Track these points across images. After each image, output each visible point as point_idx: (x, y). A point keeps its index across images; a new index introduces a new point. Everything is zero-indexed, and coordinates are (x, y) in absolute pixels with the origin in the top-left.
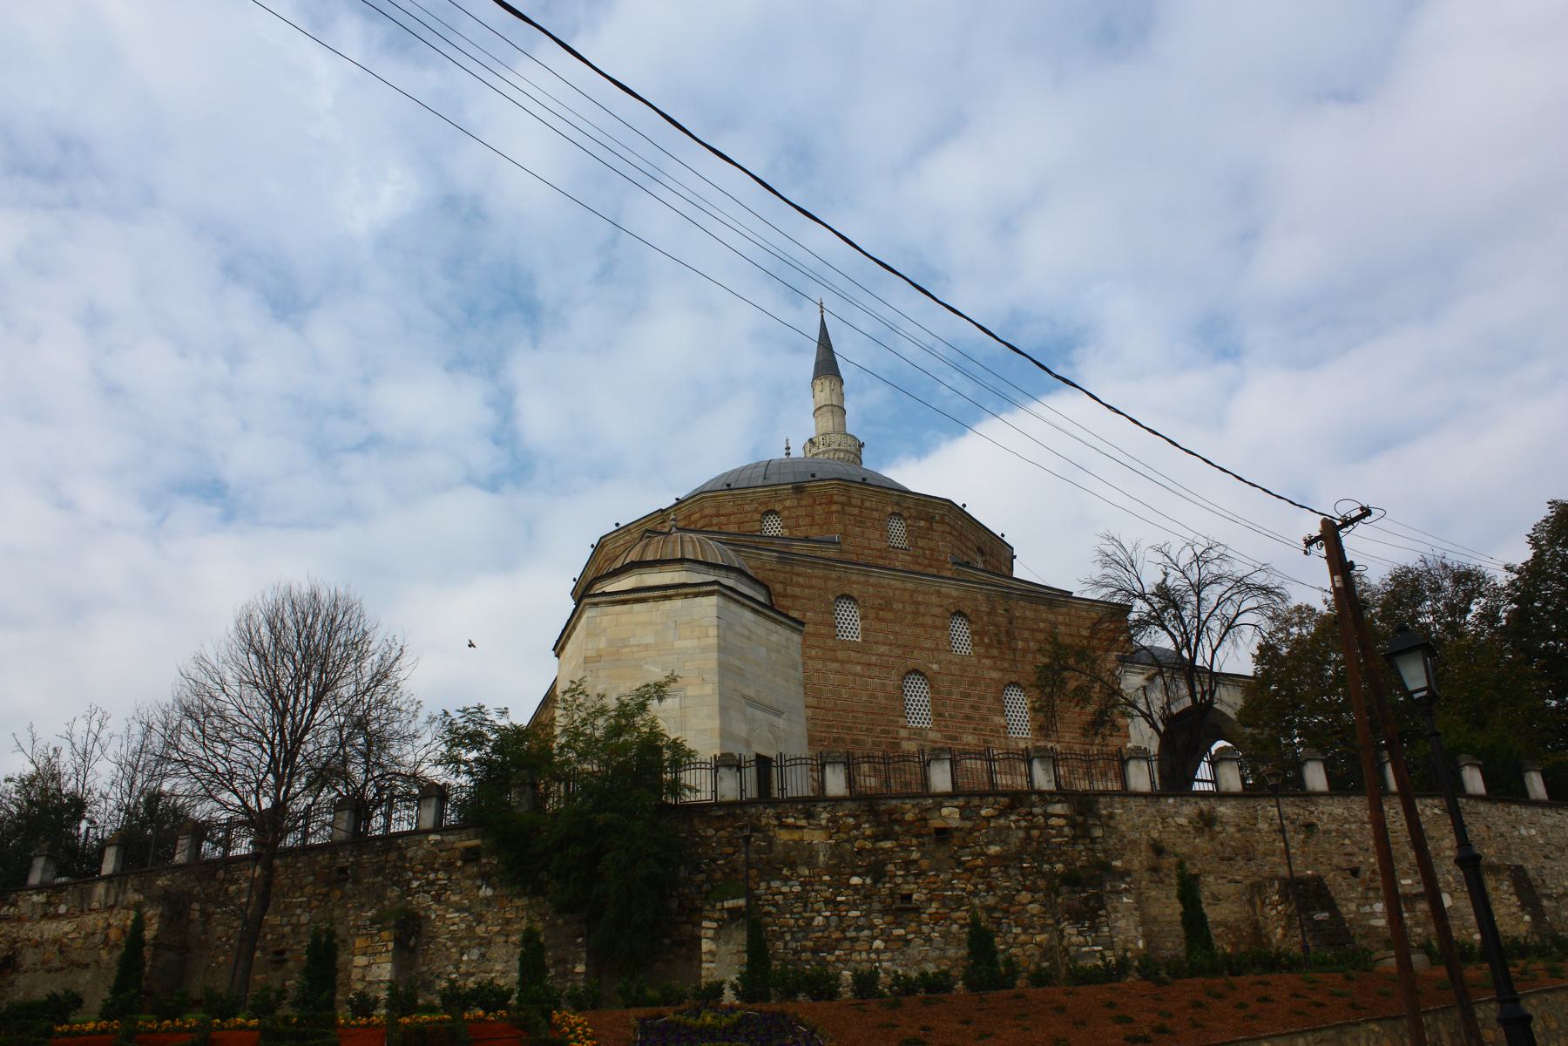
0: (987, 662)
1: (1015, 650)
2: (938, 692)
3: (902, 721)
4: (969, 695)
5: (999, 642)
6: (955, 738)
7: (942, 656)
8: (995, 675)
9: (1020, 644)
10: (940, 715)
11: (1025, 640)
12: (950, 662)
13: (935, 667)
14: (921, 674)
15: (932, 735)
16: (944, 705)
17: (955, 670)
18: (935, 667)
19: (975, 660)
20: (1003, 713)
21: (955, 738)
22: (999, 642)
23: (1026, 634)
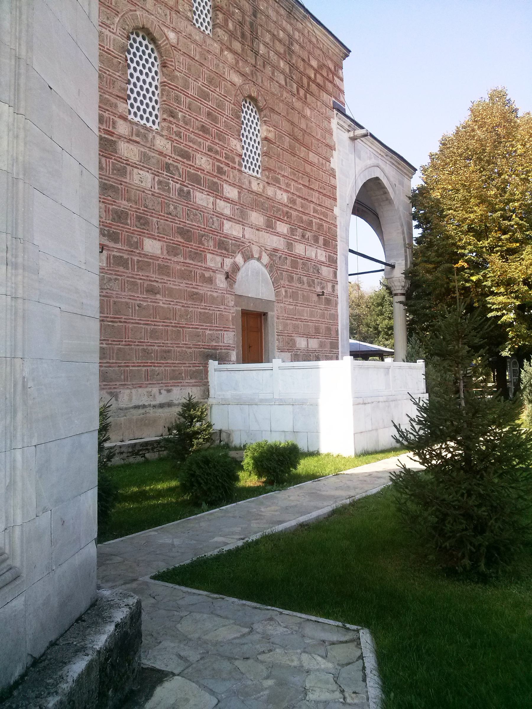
0: (229, 56)
1: (257, 53)
2: (173, 78)
3: (122, 107)
4: (205, 96)
5: (243, 35)
6: (186, 156)
7: (182, 24)
8: (237, 79)
9: (262, 50)
10: (172, 114)
11: (266, 45)
12: (189, 37)
13: (172, 36)
14: (153, 40)
15: (161, 143)
16: (177, 99)
17: (194, 51)
18: (172, 36)
19: (216, 47)
20: (239, 136)
21: (186, 156)
22: (243, 35)
23: (268, 38)
